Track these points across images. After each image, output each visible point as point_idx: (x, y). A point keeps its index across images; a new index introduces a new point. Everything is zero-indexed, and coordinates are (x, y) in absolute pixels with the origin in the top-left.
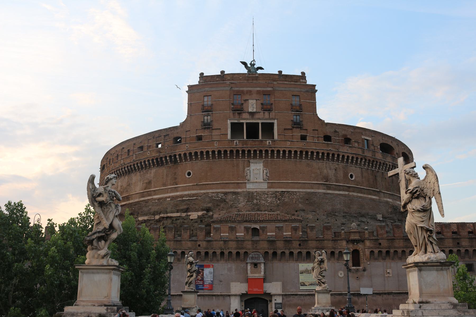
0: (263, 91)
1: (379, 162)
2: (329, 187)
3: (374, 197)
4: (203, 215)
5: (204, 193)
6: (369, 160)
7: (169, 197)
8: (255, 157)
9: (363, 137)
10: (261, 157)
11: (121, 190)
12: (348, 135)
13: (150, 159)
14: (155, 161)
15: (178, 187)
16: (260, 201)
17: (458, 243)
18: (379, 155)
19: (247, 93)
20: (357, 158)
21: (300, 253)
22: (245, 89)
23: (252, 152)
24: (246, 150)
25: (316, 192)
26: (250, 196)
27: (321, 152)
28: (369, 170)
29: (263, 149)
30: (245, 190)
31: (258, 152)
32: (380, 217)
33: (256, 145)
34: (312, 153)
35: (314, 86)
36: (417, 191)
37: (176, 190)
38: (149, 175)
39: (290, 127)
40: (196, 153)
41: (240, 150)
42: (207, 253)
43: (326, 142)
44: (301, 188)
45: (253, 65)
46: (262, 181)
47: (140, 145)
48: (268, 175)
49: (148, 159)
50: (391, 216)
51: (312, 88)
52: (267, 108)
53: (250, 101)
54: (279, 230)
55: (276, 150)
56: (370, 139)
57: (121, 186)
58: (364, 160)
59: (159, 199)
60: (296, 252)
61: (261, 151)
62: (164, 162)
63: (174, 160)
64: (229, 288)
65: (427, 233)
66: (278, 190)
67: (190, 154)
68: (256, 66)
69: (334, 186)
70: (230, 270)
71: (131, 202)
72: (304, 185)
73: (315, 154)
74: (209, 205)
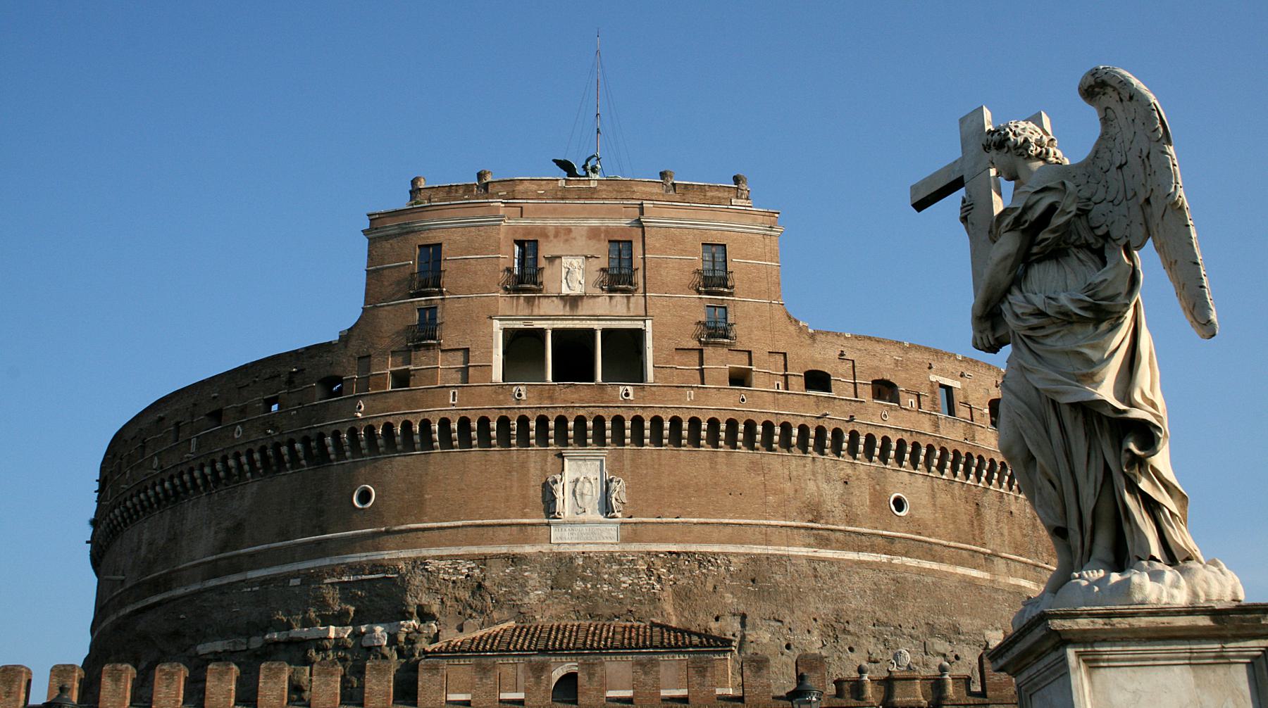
0: (608, 230)
1: (984, 455)
2: (823, 541)
6: (956, 453)
7: (296, 575)
8: (581, 440)
9: (933, 378)
10: (600, 440)
11: (151, 556)
13: (243, 450)
14: (256, 456)
15: (328, 539)
16: (594, 586)
19: (556, 236)
20: (916, 446)
22: (551, 223)
23: (571, 424)
25: (782, 556)
26: (563, 569)
27: (796, 423)
28: (956, 486)
30: (545, 548)
31: (590, 424)
33: (582, 401)
34: (768, 426)
36: (1052, 209)
37: (320, 549)
39: (694, 344)
44: (730, 541)
46: (602, 518)
47: (214, 407)
48: (624, 499)
49: (237, 449)
53: (565, 261)
54: (645, 673)
57: (150, 544)
58: (938, 453)
59: (264, 582)
61: (599, 421)
62: (286, 457)
65: (1118, 444)
66: (654, 547)
69: (840, 536)
71: (180, 591)
72: (738, 534)
73: (778, 430)
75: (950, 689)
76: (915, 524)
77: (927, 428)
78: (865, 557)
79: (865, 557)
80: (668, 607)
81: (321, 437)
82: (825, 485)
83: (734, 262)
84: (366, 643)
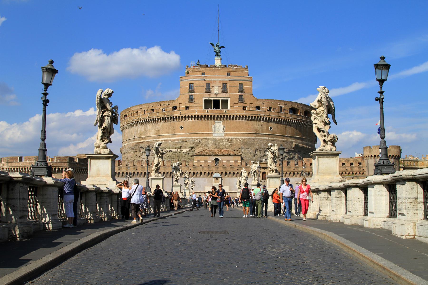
0: (223, 81)
2: (257, 135)
3: (283, 139)
4: (190, 150)
7: (171, 140)
8: (217, 119)
9: (279, 106)
18: (288, 116)
21: (238, 173)
26: (215, 141)
27: (254, 116)
29: (222, 115)
30: (212, 137)
34: (249, 116)
37: (174, 136)
38: (158, 126)
39: (237, 102)
40: (185, 117)
41: (210, 115)
42: (194, 173)
52: (224, 90)
53: (215, 87)
59: (165, 141)
61: (221, 116)
63: (173, 119)
64: (204, 190)
67: (182, 117)
68: (219, 46)
70: (205, 181)
71: (147, 140)
74: (193, 145)
81: (173, 117)
83: (244, 86)
84: (183, 152)
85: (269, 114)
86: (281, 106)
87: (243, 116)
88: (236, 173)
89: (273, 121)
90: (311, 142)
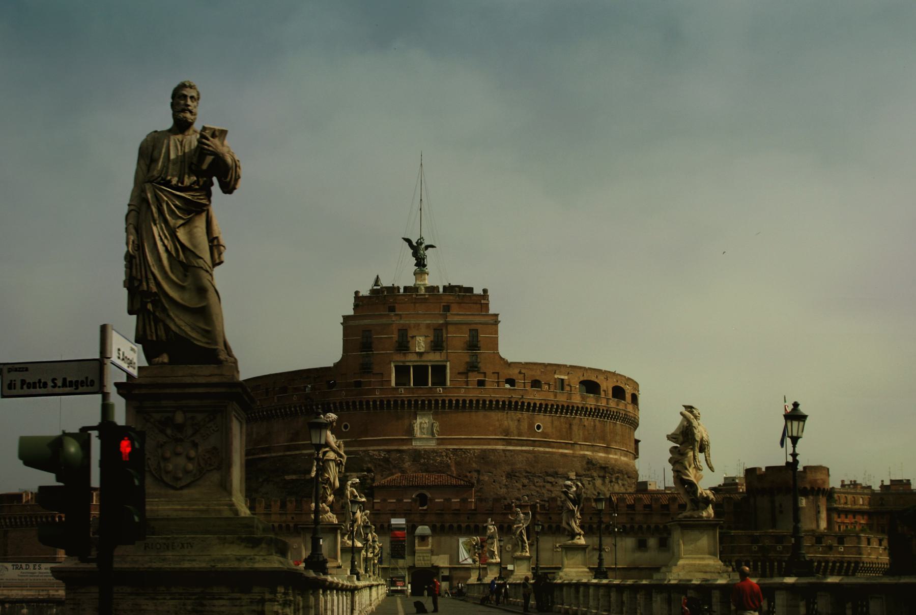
2: (509, 442)
3: (566, 451)
5: (364, 451)
6: (563, 406)
8: (423, 408)
9: (556, 376)
10: (430, 408)
12: (538, 375)
17: (632, 519)
21: (468, 527)
22: (413, 321)
24: (413, 399)
26: (417, 455)
28: (562, 420)
30: (410, 447)
32: (572, 475)
35: (497, 315)
43: (507, 386)
45: (420, 243)
50: (587, 473)
51: (494, 318)
53: (418, 338)
55: (447, 399)
56: (566, 377)
60: (464, 525)
61: (430, 401)
66: (449, 447)
68: (423, 246)
72: (479, 441)
74: (369, 465)
75: (538, 509)
76: (544, 434)
77: (552, 398)
78: (524, 448)
79: (524, 448)
80: (453, 469)
82: (511, 423)
85: (535, 396)
86: (562, 377)
87: (478, 401)
88: (464, 525)
89: (543, 408)
90: (626, 455)
